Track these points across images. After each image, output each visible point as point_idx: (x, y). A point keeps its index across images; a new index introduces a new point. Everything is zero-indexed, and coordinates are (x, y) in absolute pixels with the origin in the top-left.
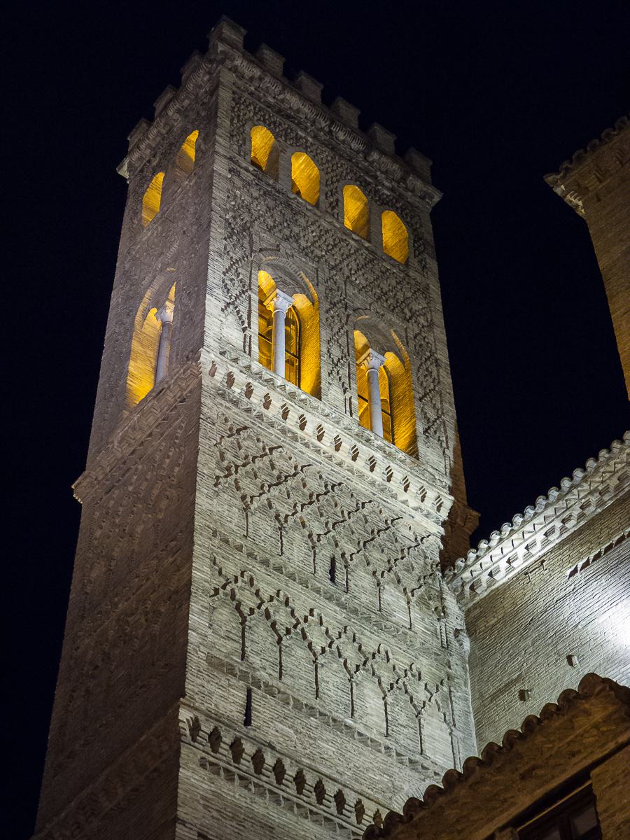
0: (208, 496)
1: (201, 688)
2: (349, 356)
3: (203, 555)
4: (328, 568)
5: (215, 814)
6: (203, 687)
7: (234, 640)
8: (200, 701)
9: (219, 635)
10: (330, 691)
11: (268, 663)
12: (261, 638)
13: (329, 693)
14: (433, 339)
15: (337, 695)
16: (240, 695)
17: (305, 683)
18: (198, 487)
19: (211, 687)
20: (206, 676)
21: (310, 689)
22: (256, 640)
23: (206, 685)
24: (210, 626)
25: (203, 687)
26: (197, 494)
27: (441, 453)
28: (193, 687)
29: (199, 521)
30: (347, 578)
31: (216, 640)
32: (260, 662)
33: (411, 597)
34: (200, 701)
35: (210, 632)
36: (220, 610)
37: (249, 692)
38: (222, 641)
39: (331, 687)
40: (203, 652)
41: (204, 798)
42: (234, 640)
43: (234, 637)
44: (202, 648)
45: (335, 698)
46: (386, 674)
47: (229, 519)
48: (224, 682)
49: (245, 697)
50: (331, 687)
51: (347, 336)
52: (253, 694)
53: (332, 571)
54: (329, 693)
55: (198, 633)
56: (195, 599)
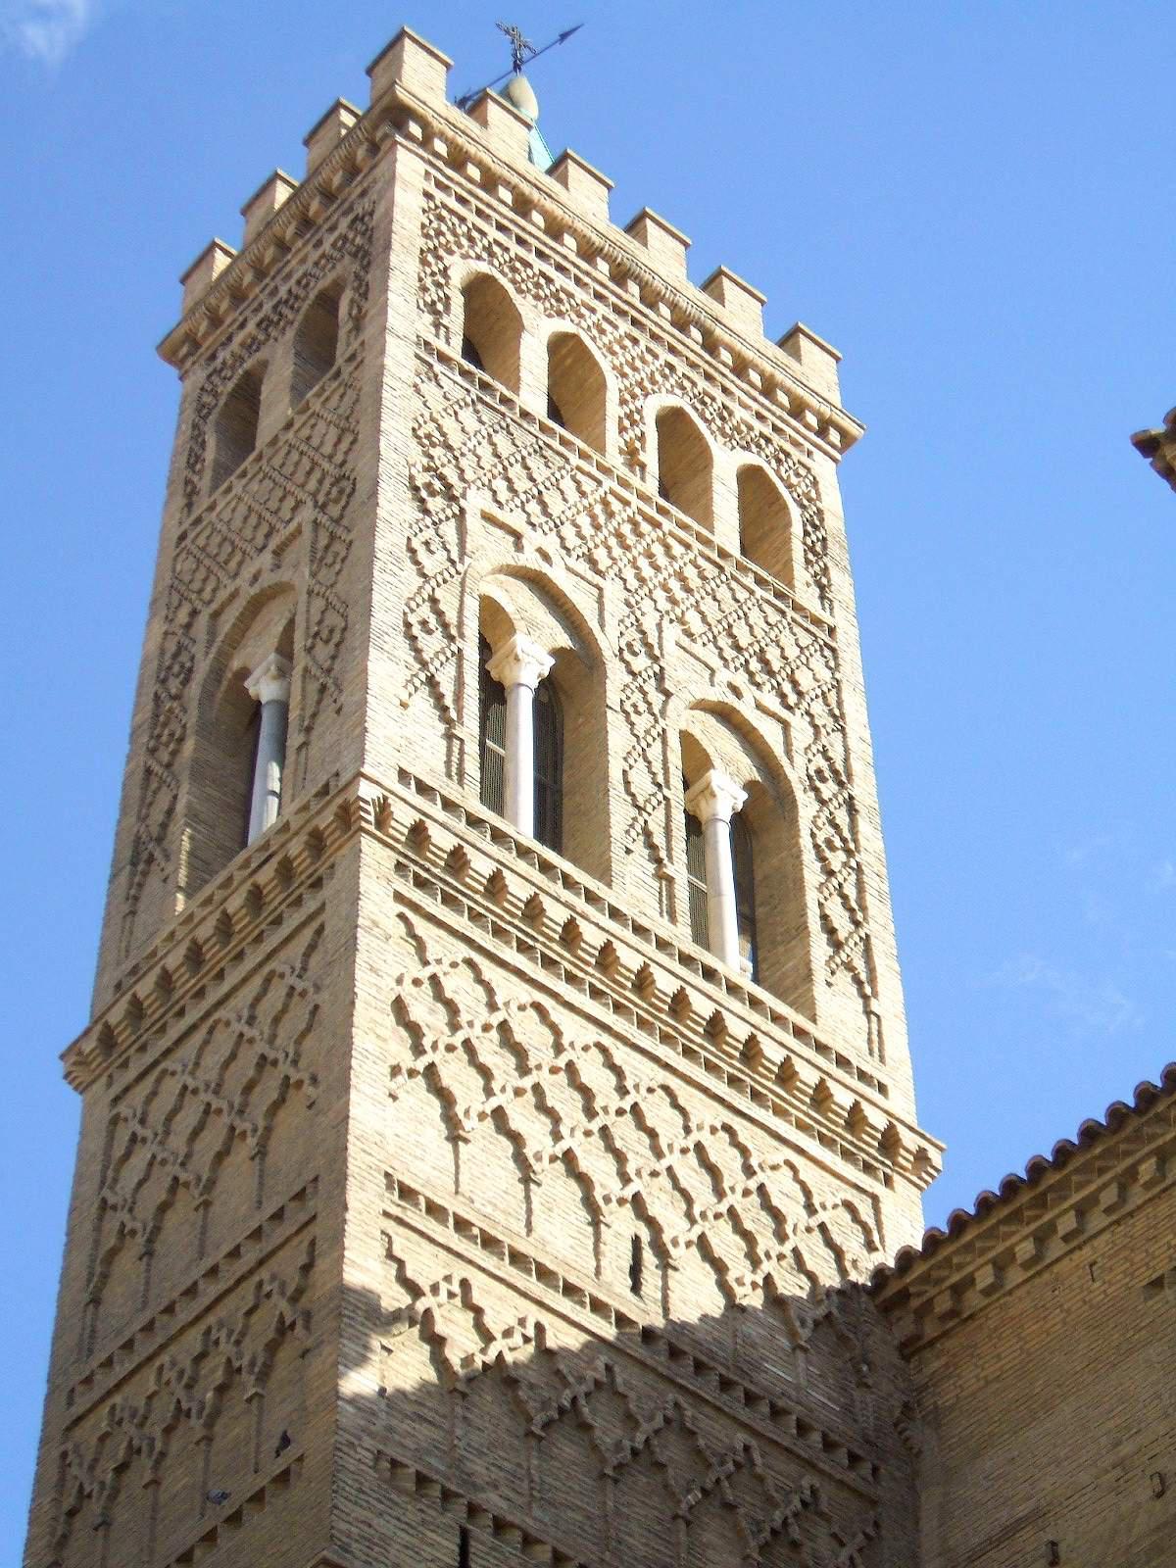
1: (366, 1528)
2: (669, 788)
3: (366, 1234)
4: (626, 1262)
6: (370, 1526)
7: (430, 1422)
8: (364, 1558)
9: (400, 1412)
10: (631, 1536)
11: (502, 1474)
12: (487, 1418)
13: (631, 1540)
14: (841, 749)
15: (646, 1545)
16: (445, 1543)
17: (579, 1518)
18: (354, 1081)
20: (375, 1503)
21: (590, 1531)
22: (478, 1422)
23: (375, 1522)
25: (370, 1526)
26: (354, 1095)
27: (861, 1008)
28: (347, 1526)
29: (358, 1160)
30: (665, 1288)
31: (394, 1422)
32: (484, 1471)
33: (800, 1330)
34: (364, 1558)
36: (402, 1356)
38: (406, 1426)
39: (634, 1527)
40: (368, 1450)
42: (430, 1422)
43: (430, 1415)
44: (368, 1442)
45: (642, 1551)
46: (748, 1498)
47: (419, 1152)
48: (412, 1517)
49: (457, 1549)
50: (634, 1527)
51: (664, 743)
52: (473, 1543)
53: (636, 1271)
54: (631, 1540)
55: (359, 1409)
56: (350, 1330)
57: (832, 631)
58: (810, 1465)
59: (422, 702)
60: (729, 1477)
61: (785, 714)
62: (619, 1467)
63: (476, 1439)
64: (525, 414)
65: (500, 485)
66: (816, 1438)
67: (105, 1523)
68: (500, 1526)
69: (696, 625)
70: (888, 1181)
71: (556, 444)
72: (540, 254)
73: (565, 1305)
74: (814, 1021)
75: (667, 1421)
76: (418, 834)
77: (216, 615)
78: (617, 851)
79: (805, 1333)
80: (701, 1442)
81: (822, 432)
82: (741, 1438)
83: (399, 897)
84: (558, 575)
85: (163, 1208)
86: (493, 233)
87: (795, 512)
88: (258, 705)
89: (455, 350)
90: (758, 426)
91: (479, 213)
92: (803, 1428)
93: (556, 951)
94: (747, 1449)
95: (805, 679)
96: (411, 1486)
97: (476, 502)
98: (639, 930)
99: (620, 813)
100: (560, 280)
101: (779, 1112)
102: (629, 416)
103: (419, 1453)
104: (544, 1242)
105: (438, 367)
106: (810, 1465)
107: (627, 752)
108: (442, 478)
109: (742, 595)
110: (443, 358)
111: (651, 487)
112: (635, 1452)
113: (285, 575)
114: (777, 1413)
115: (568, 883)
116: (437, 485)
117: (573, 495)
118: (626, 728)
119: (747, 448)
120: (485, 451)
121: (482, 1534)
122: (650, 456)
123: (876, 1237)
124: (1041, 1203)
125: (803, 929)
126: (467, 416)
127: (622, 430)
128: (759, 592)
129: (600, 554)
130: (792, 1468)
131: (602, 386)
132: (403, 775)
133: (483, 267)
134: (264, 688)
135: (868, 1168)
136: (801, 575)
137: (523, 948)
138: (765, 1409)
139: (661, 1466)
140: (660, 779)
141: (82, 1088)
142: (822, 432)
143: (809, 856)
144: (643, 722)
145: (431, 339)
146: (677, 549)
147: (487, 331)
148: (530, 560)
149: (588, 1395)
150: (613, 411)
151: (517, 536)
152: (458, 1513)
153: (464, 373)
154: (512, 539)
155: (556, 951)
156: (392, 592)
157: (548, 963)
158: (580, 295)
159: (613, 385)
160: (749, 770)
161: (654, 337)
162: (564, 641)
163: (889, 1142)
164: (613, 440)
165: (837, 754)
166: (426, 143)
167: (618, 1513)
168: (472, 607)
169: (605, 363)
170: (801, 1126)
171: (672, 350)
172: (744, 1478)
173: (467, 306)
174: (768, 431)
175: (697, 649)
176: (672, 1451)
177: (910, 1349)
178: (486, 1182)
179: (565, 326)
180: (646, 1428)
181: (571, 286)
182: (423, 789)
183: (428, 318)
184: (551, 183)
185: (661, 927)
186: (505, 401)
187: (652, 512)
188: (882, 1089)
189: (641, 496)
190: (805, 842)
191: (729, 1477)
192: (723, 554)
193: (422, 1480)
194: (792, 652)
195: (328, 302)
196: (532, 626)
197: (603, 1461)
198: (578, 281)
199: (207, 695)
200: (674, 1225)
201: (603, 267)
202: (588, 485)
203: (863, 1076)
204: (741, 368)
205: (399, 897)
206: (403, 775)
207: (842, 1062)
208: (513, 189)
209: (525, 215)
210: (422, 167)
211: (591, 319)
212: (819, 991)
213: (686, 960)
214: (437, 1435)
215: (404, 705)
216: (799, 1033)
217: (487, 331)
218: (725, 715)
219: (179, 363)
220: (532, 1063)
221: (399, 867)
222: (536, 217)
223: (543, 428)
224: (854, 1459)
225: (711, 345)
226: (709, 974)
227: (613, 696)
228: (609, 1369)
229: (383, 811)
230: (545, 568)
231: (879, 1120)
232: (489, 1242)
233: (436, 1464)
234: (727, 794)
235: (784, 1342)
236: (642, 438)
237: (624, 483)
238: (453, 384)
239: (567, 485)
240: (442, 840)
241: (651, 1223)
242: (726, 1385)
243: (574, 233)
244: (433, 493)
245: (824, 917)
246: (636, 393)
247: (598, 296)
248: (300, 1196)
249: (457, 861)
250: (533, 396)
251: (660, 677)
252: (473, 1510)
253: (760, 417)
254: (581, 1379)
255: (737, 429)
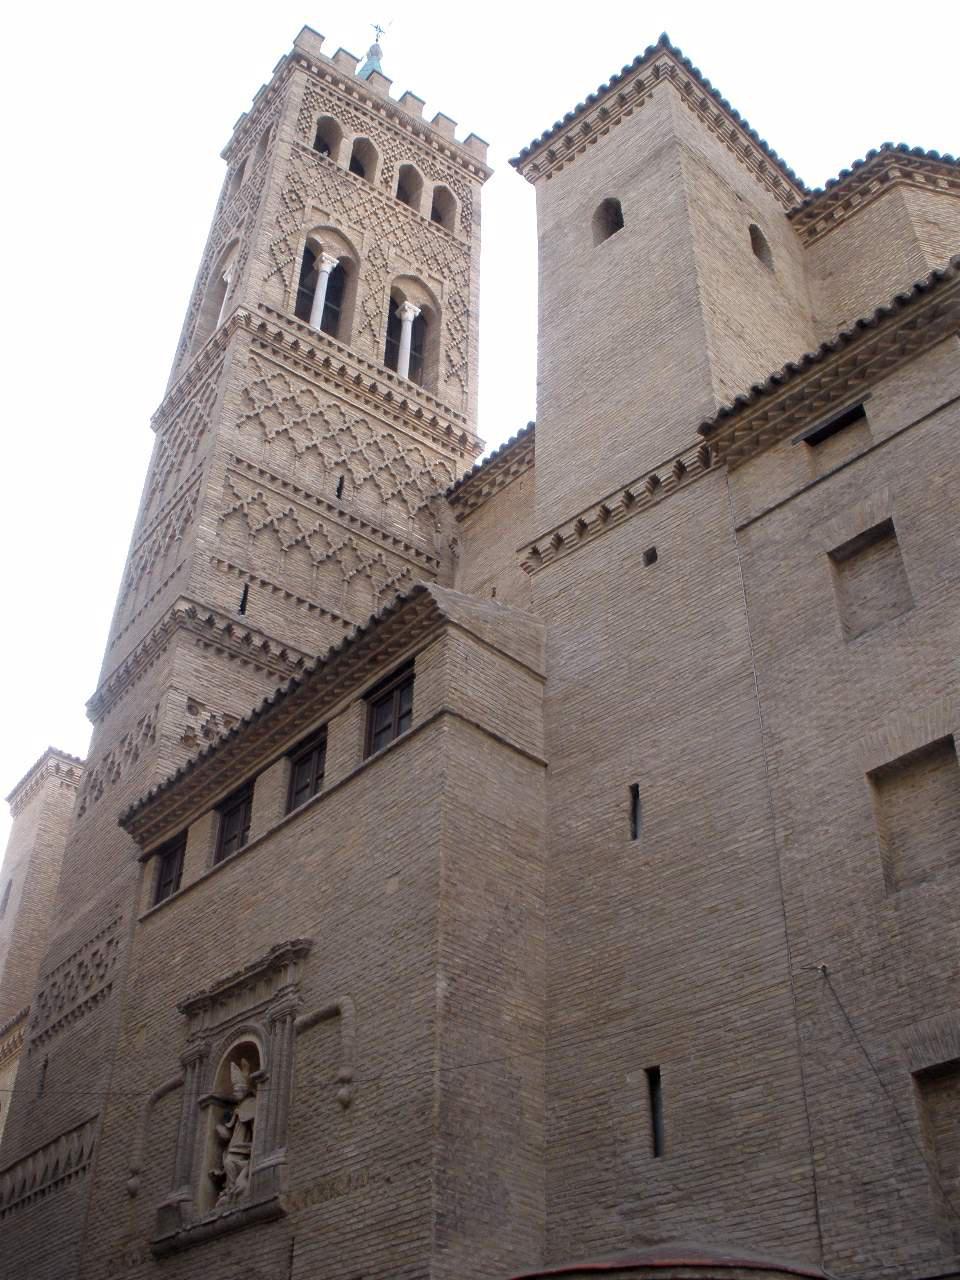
0: (230, 428)
5: (205, 683)
19: (213, 585)
24: (218, 535)
35: (218, 539)
37: (247, 587)
41: (196, 670)
53: (340, 490)
57: (469, 248)
58: (408, 561)
59: (274, 279)
60: (370, 566)
61: (442, 279)
62: (320, 562)
63: (258, 552)
64: (339, 169)
65: (324, 197)
66: (413, 552)
67: (137, 589)
68: (264, 584)
69: (405, 245)
70: (462, 455)
71: (351, 179)
72: (356, 109)
73: (305, 503)
74: (436, 395)
75: (345, 545)
76: (263, 327)
77: (219, 252)
78: (354, 332)
79: (414, 512)
80: (359, 553)
81: (476, 173)
82: (378, 551)
83: (252, 351)
84: (344, 229)
85: (169, 472)
86: (334, 100)
87: (459, 204)
88: (225, 284)
89: (310, 145)
90: (447, 171)
91: (331, 94)
92: (407, 548)
93: (321, 370)
94: (380, 555)
95: (454, 267)
96: (226, 569)
97: (310, 202)
98: (360, 362)
99: (357, 321)
100: (363, 118)
101: (415, 429)
102: (387, 169)
103: (230, 558)
104: (300, 479)
105: (301, 153)
106: (408, 561)
107: (367, 299)
108: (297, 195)
109: (428, 235)
110: (304, 149)
111: (394, 194)
112: (328, 556)
113: (238, 235)
114: (396, 542)
115: (330, 344)
116: (294, 197)
117: (356, 200)
118: (366, 287)
119: (441, 179)
120: (318, 185)
121: (255, 587)
122: (395, 185)
123: (453, 476)
124: (505, 461)
125: (437, 360)
126: (313, 172)
127: (383, 173)
128: (437, 234)
129: (366, 222)
130: (401, 562)
131: (377, 158)
132: (260, 306)
133: (329, 115)
134: (229, 278)
135: (453, 450)
136: (458, 225)
137: (306, 369)
138: (391, 540)
139: (340, 562)
140: (380, 304)
141: (156, 431)
142: (476, 173)
143: (444, 333)
144: (374, 286)
145: (301, 143)
146: (401, 218)
147: (326, 140)
148: (332, 223)
149: (310, 536)
150: (380, 165)
151: (328, 215)
152: (246, 579)
153: (313, 155)
154: (326, 217)
155: (321, 370)
156: (266, 238)
157: (317, 374)
158: (371, 123)
159: (381, 157)
160: (424, 299)
161: (404, 139)
162: (344, 253)
163: (463, 439)
164: (378, 176)
165: (464, 292)
166: (309, 68)
167: (317, 579)
168: (303, 241)
169: (379, 150)
170: (425, 434)
171: (412, 143)
172: (378, 566)
173: (319, 130)
174: (452, 172)
175: (404, 255)
176: (346, 557)
177: (460, 518)
178: (279, 456)
179: (363, 135)
180: (335, 547)
181: (367, 120)
182: (269, 311)
183: (301, 134)
184: (367, 83)
185: (373, 360)
186: (330, 165)
187: (393, 205)
188: (464, 420)
189: (388, 199)
190: (443, 326)
191: (370, 566)
192: (422, 219)
193: (231, 567)
194: (450, 256)
195: (268, 131)
196: (331, 247)
197: (313, 560)
198: (372, 119)
199: (212, 282)
200: (360, 473)
201: (383, 113)
202: (363, 195)
203: (456, 416)
204: (441, 149)
205: (252, 351)
206: (260, 306)
207: (447, 410)
208: (346, 84)
209: (351, 94)
210: (306, 77)
211: (375, 132)
212: (441, 385)
213: (380, 372)
214: (239, 550)
215: (265, 280)
216: (429, 399)
217: (326, 140)
218: (415, 280)
219: (227, 159)
220: (304, 412)
221: (254, 340)
222: (355, 94)
223: (347, 174)
224: (429, 559)
225: (428, 140)
226: (390, 378)
227: (362, 274)
228: (321, 525)
229: (248, 319)
230: (339, 227)
231: (459, 433)
232: (273, 479)
233: (238, 563)
234: (411, 312)
235: (405, 516)
236: (392, 177)
237: (381, 194)
238: (308, 159)
239: (355, 196)
240: (272, 329)
241: (349, 470)
242: (374, 531)
243: (370, 99)
244: (293, 201)
245: (448, 356)
246: (390, 158)
247: (381, 124)
248: (200, 465)
249: (279, 336)
250: (344, 162)
251: (385, 266)
252: (253, 578)
253: (449, 168)
254: (307, 530)
255: (437, 172)
